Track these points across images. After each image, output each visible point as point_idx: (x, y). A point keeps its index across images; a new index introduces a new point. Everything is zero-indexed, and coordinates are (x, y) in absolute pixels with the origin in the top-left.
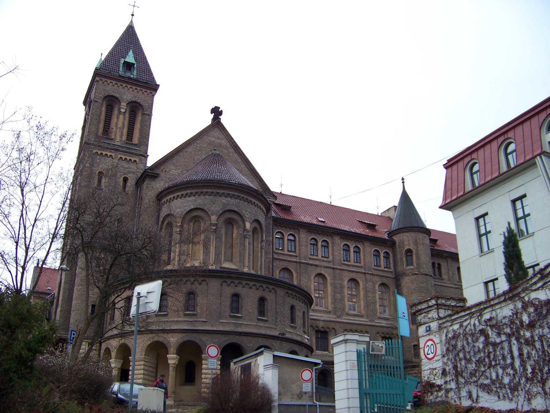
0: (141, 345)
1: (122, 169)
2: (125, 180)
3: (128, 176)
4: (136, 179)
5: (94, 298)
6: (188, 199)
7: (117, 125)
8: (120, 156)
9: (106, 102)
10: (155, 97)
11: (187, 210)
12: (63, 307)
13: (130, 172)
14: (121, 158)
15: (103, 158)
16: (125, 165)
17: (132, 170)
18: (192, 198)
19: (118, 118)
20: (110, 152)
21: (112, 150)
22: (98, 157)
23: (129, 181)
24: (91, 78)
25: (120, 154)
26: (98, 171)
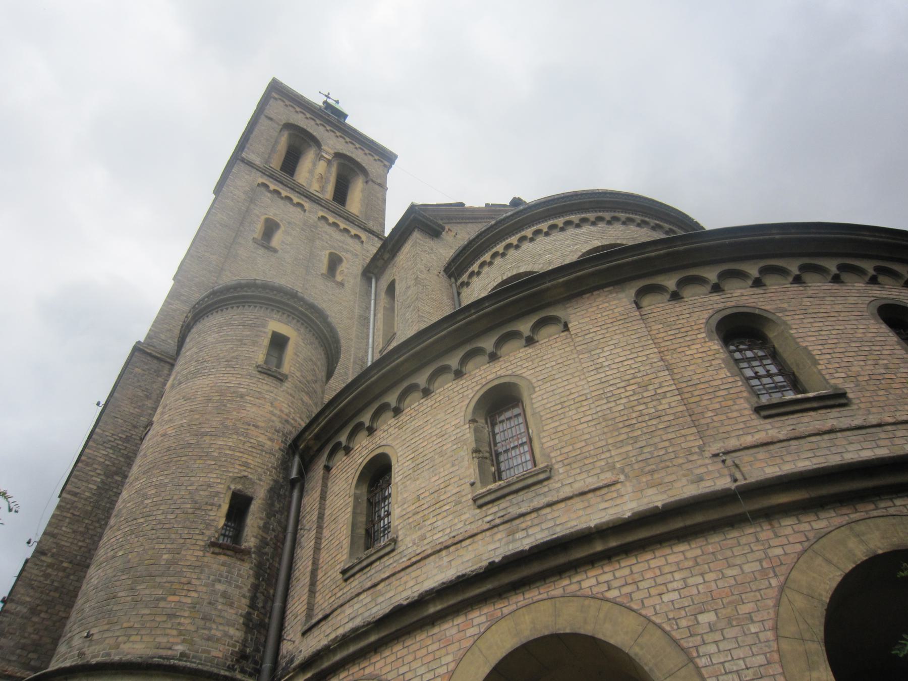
0: (744, 609)
1: (327, 237)
2: (334, 262)
3: (342, 254)
4: (363, 266)
5: (246, 465)
6: (571, 231)
7: (311, 172)
8: (321, 214)
9: (290, 135)
10: (389, 175)
11: (584, 251)
12: (54, 536)
13: (347, 251)
14: (324, 218)
15: (281, 203)
16: (337, 235)
17: (351, 249)
18: (586, 229)
19: (314, 165)
20: (298, 197)
21: (302, 197)
22: (269, 195)
23: (343, 267)
24: (255, 108)
25: (322, 211)
26: (267, 216)
